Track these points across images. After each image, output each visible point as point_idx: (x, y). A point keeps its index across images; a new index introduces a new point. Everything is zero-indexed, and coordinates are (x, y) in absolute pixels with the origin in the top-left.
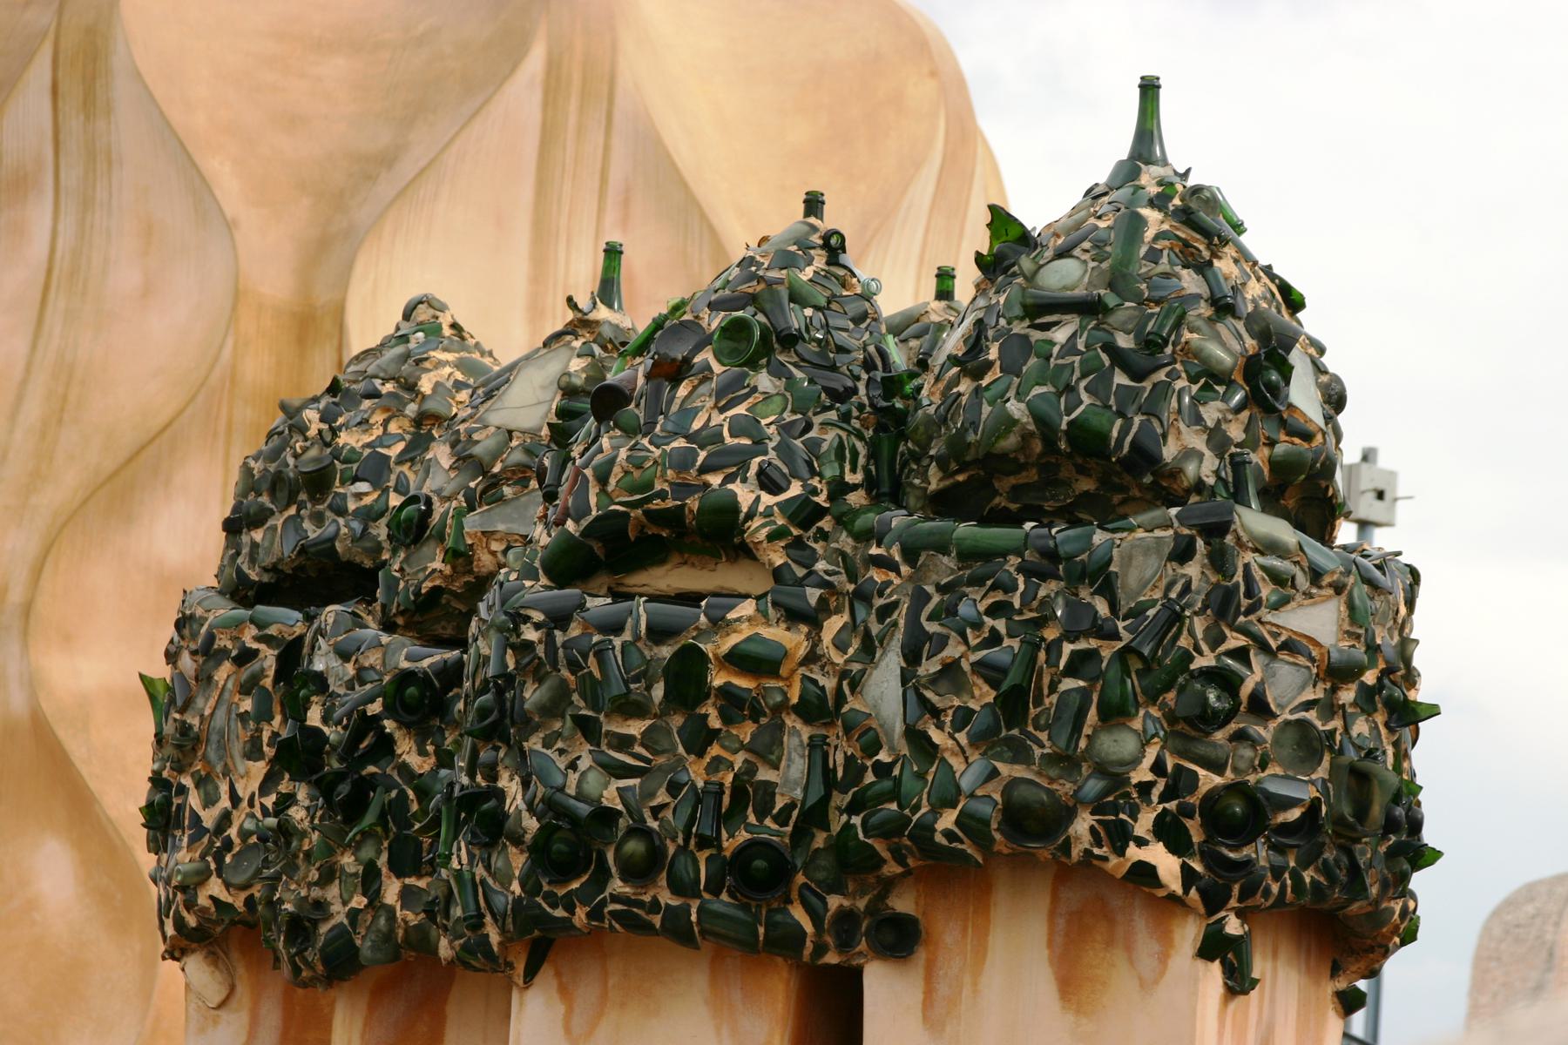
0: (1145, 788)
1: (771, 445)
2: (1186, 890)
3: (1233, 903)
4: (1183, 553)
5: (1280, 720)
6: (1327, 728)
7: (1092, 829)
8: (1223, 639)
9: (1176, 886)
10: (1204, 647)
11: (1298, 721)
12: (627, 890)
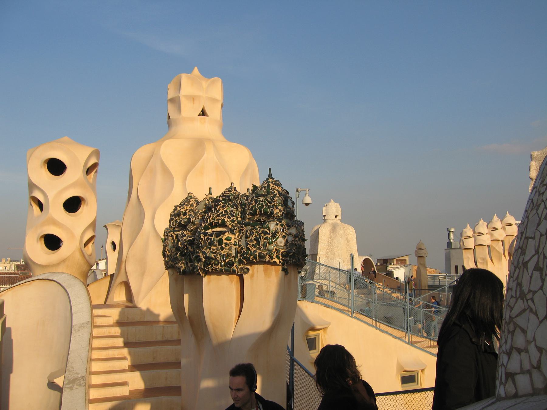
0: (274, 252)
4: (277, 225)
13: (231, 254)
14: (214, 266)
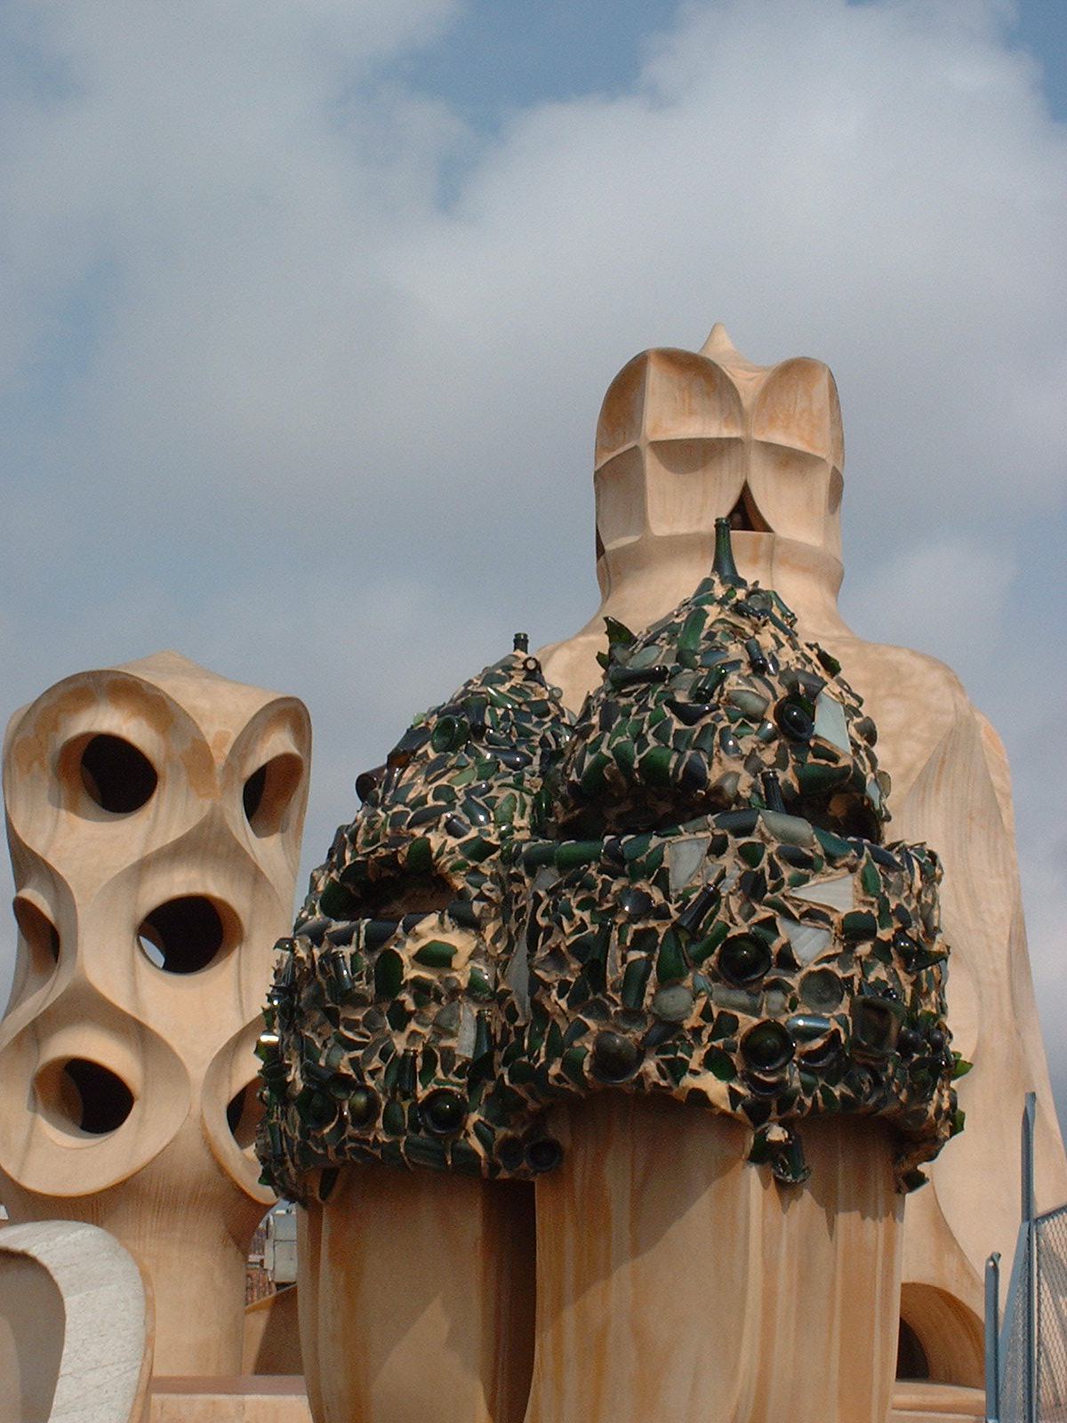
0: (697, 1032)
1: (459, 803)
2: (734, 1108)
3: (774, 1115)
4: (718, 848)
5: (804, 972)
6: (847, 975)
7: (658, 1065)
8: (753, 912)
9: (726, 1106)
10: (739, 919)
11: (820, 971)
12: (357, 1132)
13: (449, 1053)
14: (351, 1130)
